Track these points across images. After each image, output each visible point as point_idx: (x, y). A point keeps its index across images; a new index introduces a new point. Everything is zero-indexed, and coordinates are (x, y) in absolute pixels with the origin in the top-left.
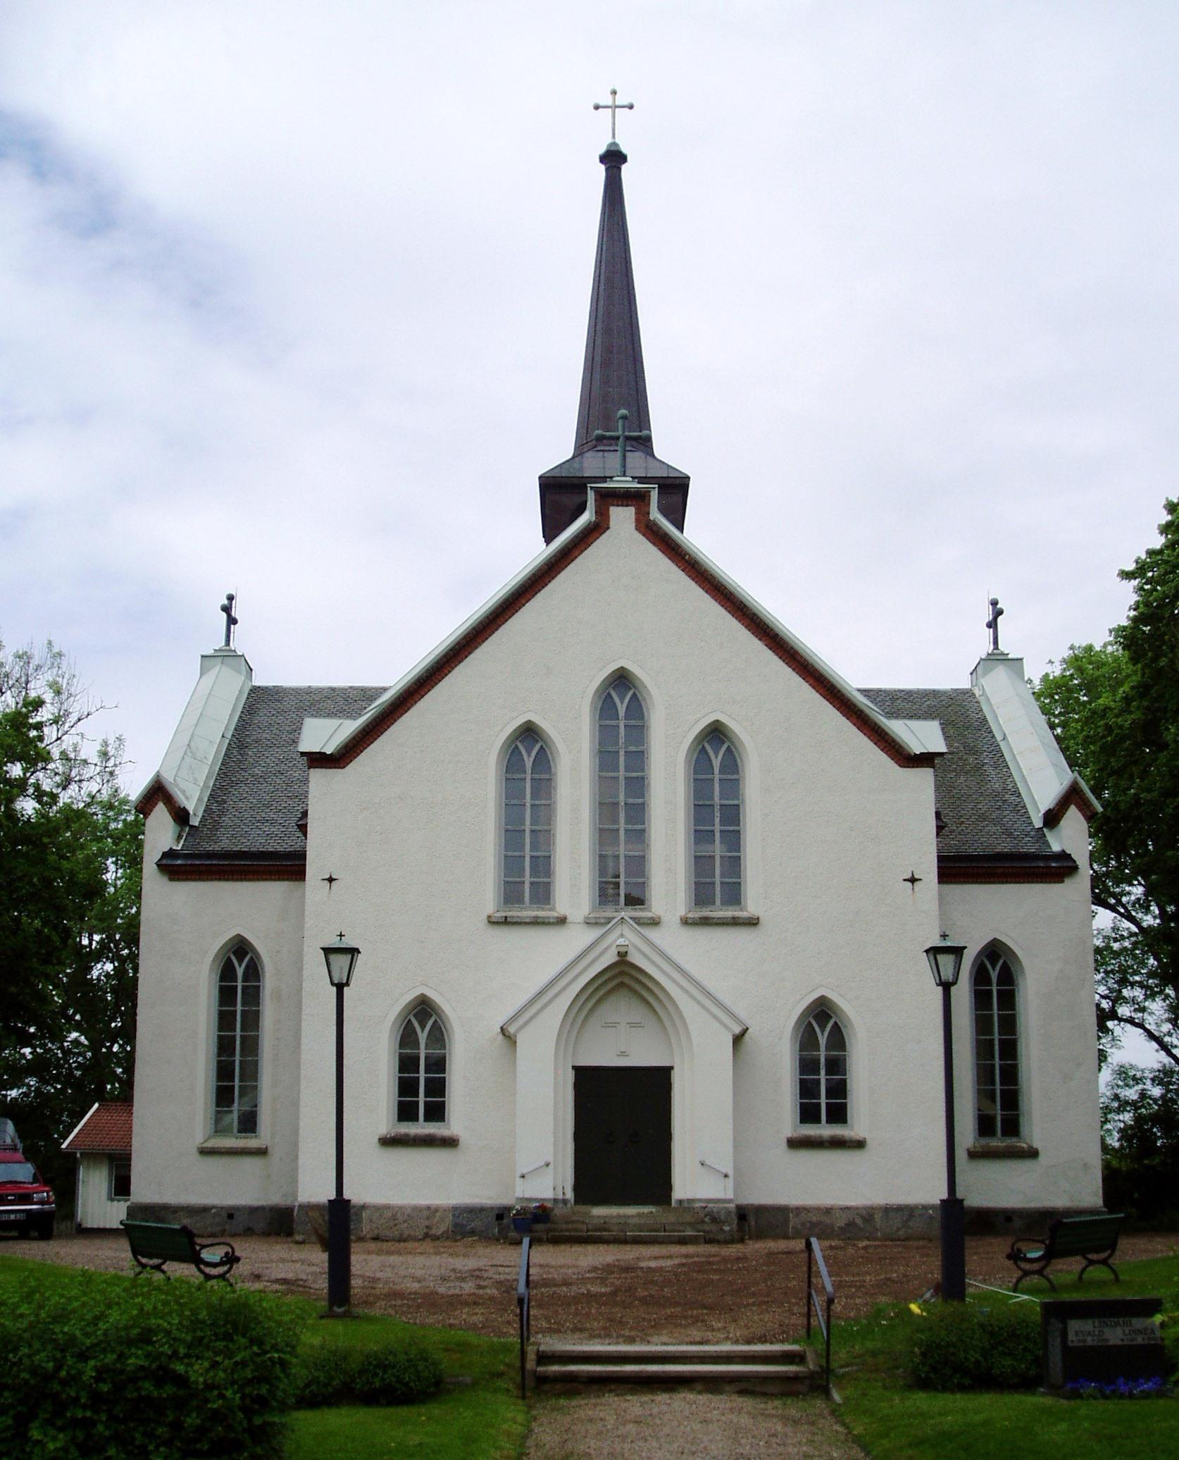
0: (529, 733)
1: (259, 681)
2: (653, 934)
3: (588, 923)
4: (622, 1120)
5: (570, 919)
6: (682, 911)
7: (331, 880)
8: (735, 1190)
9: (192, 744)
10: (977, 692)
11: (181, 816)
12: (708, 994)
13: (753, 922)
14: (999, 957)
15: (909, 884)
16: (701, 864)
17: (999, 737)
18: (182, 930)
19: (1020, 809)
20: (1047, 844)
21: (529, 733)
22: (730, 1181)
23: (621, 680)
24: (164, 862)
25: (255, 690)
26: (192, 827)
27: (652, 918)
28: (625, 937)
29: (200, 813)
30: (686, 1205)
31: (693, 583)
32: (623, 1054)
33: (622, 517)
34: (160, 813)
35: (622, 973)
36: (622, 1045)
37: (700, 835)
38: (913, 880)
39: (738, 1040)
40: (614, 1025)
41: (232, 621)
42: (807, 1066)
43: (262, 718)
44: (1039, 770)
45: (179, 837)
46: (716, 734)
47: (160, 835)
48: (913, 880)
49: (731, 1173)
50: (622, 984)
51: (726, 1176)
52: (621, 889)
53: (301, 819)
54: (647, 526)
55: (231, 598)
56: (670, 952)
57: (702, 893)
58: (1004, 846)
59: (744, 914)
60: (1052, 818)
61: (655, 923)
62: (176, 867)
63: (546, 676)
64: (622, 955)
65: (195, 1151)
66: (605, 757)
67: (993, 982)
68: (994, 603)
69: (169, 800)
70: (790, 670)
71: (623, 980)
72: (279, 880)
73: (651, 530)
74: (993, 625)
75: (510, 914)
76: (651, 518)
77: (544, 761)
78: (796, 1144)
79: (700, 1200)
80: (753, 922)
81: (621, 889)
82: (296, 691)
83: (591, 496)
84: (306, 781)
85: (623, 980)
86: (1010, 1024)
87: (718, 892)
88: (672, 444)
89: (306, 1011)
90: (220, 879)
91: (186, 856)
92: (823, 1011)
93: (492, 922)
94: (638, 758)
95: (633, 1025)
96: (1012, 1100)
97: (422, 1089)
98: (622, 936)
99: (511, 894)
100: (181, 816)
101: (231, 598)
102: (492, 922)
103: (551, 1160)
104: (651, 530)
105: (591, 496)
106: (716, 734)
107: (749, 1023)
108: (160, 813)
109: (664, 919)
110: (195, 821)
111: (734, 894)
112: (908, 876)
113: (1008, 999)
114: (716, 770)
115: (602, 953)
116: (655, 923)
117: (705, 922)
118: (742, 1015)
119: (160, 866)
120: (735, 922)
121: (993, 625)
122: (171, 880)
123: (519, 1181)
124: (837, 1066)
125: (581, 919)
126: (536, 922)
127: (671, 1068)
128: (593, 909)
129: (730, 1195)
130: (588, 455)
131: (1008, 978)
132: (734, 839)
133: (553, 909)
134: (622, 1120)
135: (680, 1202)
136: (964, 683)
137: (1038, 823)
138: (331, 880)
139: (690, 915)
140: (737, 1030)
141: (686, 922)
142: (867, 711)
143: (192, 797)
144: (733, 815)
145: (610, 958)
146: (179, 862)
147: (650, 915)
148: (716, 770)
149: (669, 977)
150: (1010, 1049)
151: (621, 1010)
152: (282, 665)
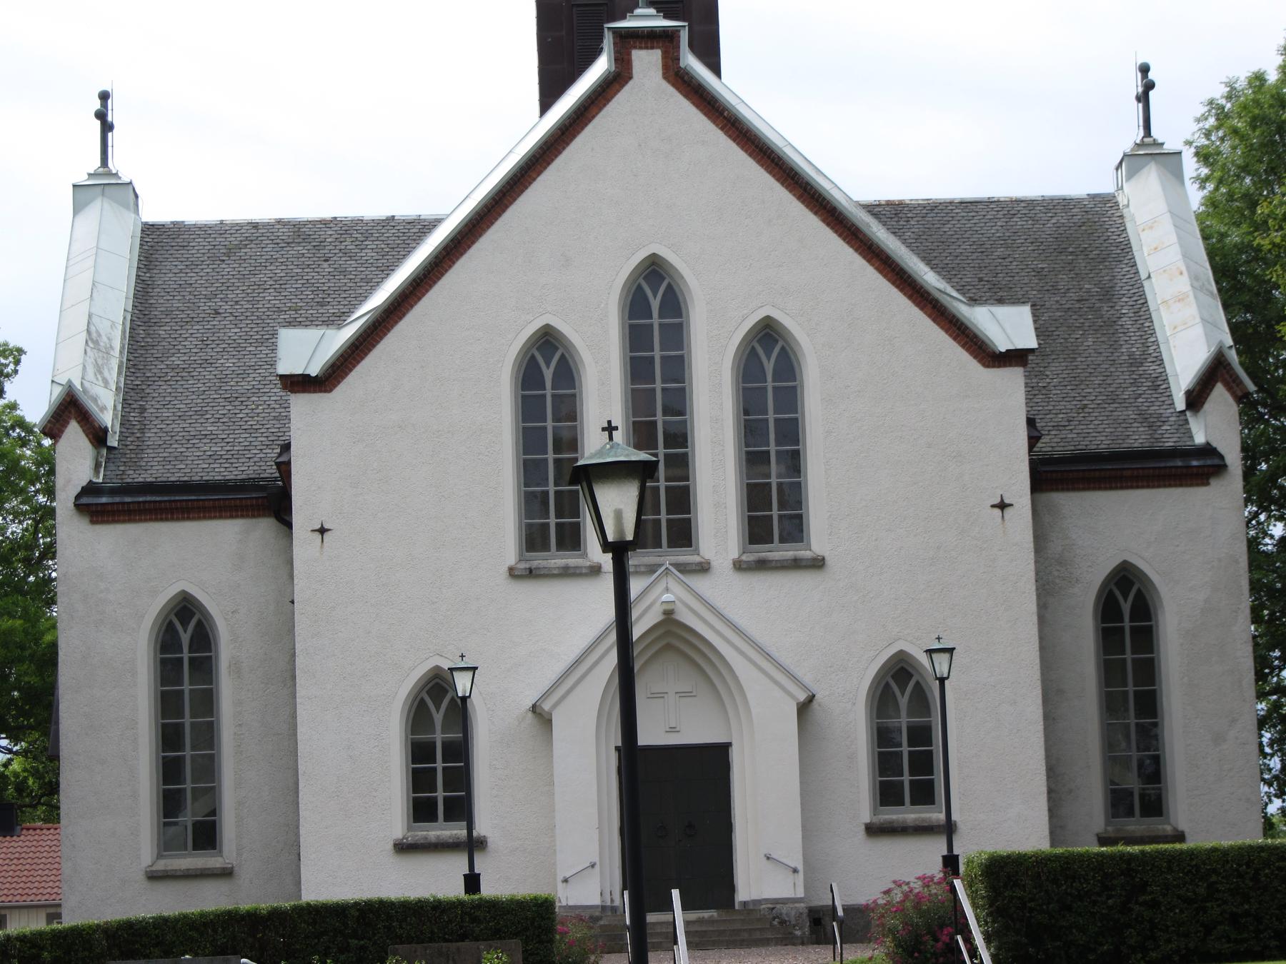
0: (547, 343)
1: (156, 211)
2: (700, 584)
4: (674, 810)
6: (734, 554)
7: (322, 531)
8: (806, 888)
9: (93, 329)
10: (1122, 200)
11: (98, 436)
12: (768, 656)
13: (818, 564)
14: (1132, 584)
15: (997, 512)
16: (755, 497)
17: (1143, 275)
19: (1160, 383)
20: (1191, 437)
22: (801, 875)
24: (84, 500)
25: (150, 230)
26: (111, 449)
27: (700, 563)
29: (117, 429)
32: (673, 730)
33: (647, 62)
35: (668, 633)
37: (753, 460)
38: (1002, 506)
39: (804, 708)
41: (107, 127)
42: (883, 736)
44: (1188, 330)
45: (97, 466)
47: (76, 463)
48: (1002, 506)
49: (800, 868)
50: (669, 647)
51: (795, 871)
53: (280, 455)
55: (104, 97)
56: (719, 603)
57: (757, 531)
58: (1138, 439)
59: (806, 554)
61: (703, 568)
62: (100, 505)
64: (668, 613)
65: (141, 876)
66: (638, 369)
67: (1127, 610)
68: (1144, 69)
70: (851, 250)
73: (682, 78)
74: (1144, 98)
75: (535, 564)
76: (682, 65)
77: (568, 373)
78: (873, 830)
79: (767, 900)
80: (818, 564)
83: (608, 42)
84: (284, 419)
86: (1148, 671)
87: (774, 515)
89: (301, 692)
90: (156, 520)
91: (113, 491)
92: (902, 669)
94: (678, 368)
96: (1154, 771)
97: (440, 771)
98: (667, 590)
100: (98, 436)
101: (104, 97)
102: (513, 573)
103: (597, 860)
105: (608, 42)
107: (815, 688)
109: (714, 564)
110: (113, 441)
111: (795, 529)
112: (997, 501)
113: (1146, 637)
114: (769, 378)
116: (703, 568)
117: (762, 565)
118: (807, 679)
120: (797, 565)
121: (1144, 98)
122: (93, 522)
123: (560, 886)
126: (567, 573)
127: (728, 745)
129: (800, 893)
131: (1144, 609)
132: (794, 462)
133: (585, 555)
134: (674, 810)
135: (745, 903)
136: (1105, 185)
137: (1180, 404)
139: (744, 558)
140: (802, 697)
141: (739, 566)
142: (944, 300)
143: (106, 404)
144: (791, 432)
146: (104, 500)
147: (696, 559)
148: (769, 378)
150: (1149, 704)
152: (186, 192)
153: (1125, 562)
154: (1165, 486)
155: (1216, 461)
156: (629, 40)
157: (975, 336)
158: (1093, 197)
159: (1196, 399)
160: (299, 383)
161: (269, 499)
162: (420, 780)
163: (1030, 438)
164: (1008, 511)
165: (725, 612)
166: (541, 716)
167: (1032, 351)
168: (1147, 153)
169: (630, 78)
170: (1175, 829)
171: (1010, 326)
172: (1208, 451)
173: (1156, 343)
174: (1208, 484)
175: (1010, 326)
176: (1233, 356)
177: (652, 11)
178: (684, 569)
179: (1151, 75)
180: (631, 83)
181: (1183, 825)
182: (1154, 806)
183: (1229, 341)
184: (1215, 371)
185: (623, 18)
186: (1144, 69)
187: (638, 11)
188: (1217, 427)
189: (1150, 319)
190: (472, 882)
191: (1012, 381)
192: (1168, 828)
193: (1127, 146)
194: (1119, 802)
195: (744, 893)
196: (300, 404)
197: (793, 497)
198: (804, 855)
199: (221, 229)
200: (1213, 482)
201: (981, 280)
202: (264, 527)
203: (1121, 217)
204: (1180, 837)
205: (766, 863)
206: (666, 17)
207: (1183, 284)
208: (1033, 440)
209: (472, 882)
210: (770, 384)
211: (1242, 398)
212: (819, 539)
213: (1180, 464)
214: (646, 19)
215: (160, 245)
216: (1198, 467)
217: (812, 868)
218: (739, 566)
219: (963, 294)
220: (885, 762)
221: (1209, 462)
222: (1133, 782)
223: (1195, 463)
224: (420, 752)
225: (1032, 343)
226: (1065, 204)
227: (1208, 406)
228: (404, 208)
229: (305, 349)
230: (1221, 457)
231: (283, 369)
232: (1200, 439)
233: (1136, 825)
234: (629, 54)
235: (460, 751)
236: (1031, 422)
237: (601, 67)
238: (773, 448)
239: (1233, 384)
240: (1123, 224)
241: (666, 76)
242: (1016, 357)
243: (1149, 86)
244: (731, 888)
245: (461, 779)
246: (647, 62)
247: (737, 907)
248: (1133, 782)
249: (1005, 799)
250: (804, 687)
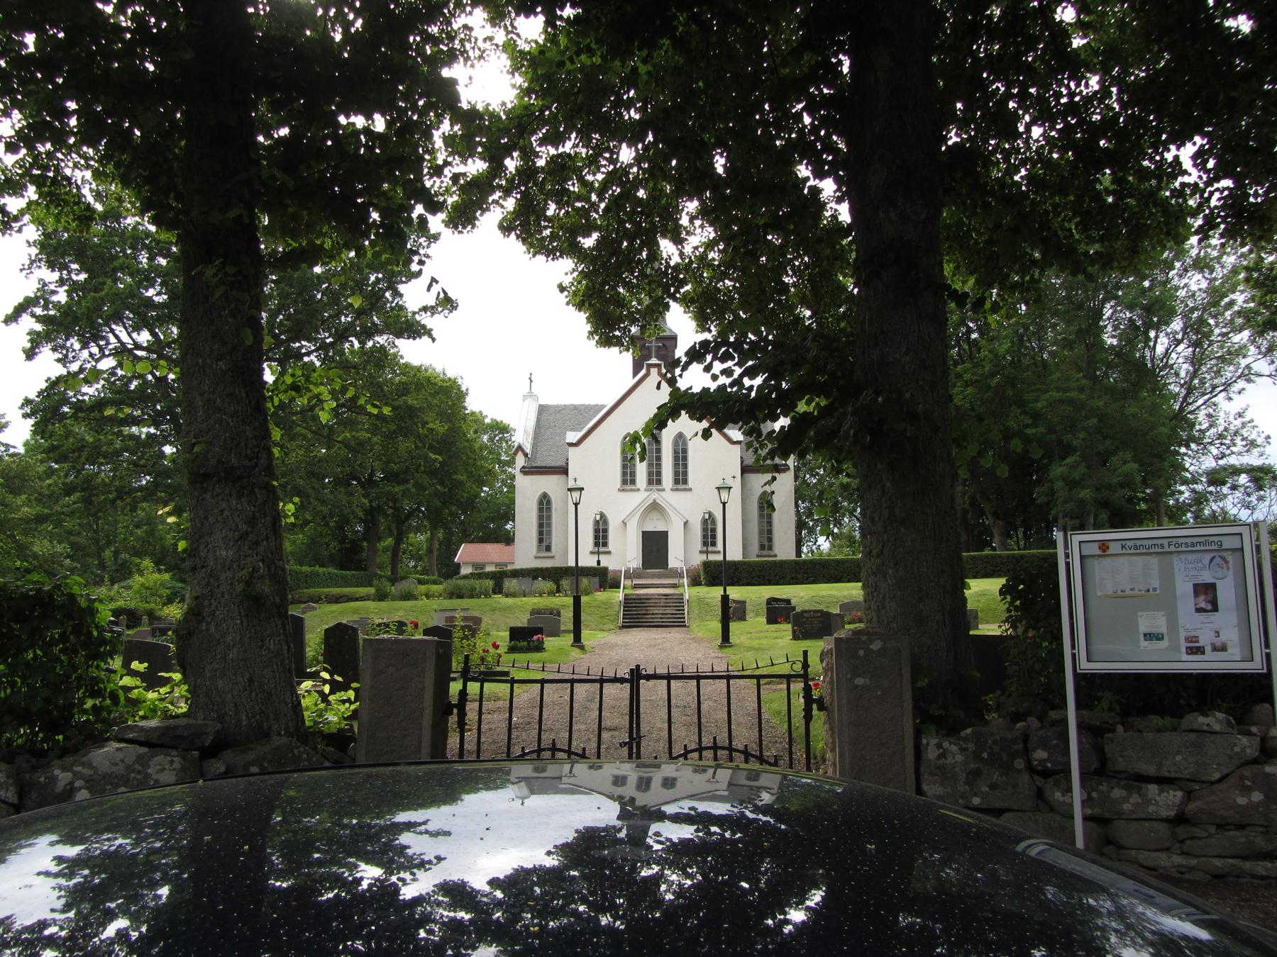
1: (542, 402)
4: (654, 546)
11: (526, 455)
16: (676, 473)
18: (528, 490)
25: (540, 406)
28: (655, 496)
33: (654, 371)
34: (520, 453)
36: (655, 525)
37: (676, 465)
39: (686, 523)
42: (705, 530)
43: (544, 417)
47: (520, 461)
52: (655, 478)
57: (676, 482)
62: (526, 471)
67: (766, 504)
69: (523, 451)
71: (655, 507)
81: (655, 478)
82: (554, 406)
85: (655, 507)
87: (681, 478)
96: (770, 540)
97: (601, 536)
99: (624, 482)
100: (526, 455)
108: (520, 453)
111: (685, 482)
126: (632, 490)
132: (685, 466)
134: (654, 546)
143: (528, 449)
151: (655, 515)
156: (650, 366)
160: (571, 445)
161: (563, 471)
162: (596, 537)
166: (625, 524)
182: (770, 548)
190: (599, 562)
191: (737, 448)
194: (762, 547)
196: (571, 449)
197: (685, 474)
199: (557, 406)
202: (564, 477)
205: (676, 558)
209: (599, 562)
212: (691, 484)
214: (654, 361)
215: (542, 409)
220: (705, 537)
222: (766, 543)
224: (596, 531)
228: (600, 403)
229: (572, 437)
231: (568, 440)
233: (765, 552)
235: (605, 531)
237: (643, 372)
242: (739, 442)
245: (605, 537)
246: (654, 371)
248: (766, 543)
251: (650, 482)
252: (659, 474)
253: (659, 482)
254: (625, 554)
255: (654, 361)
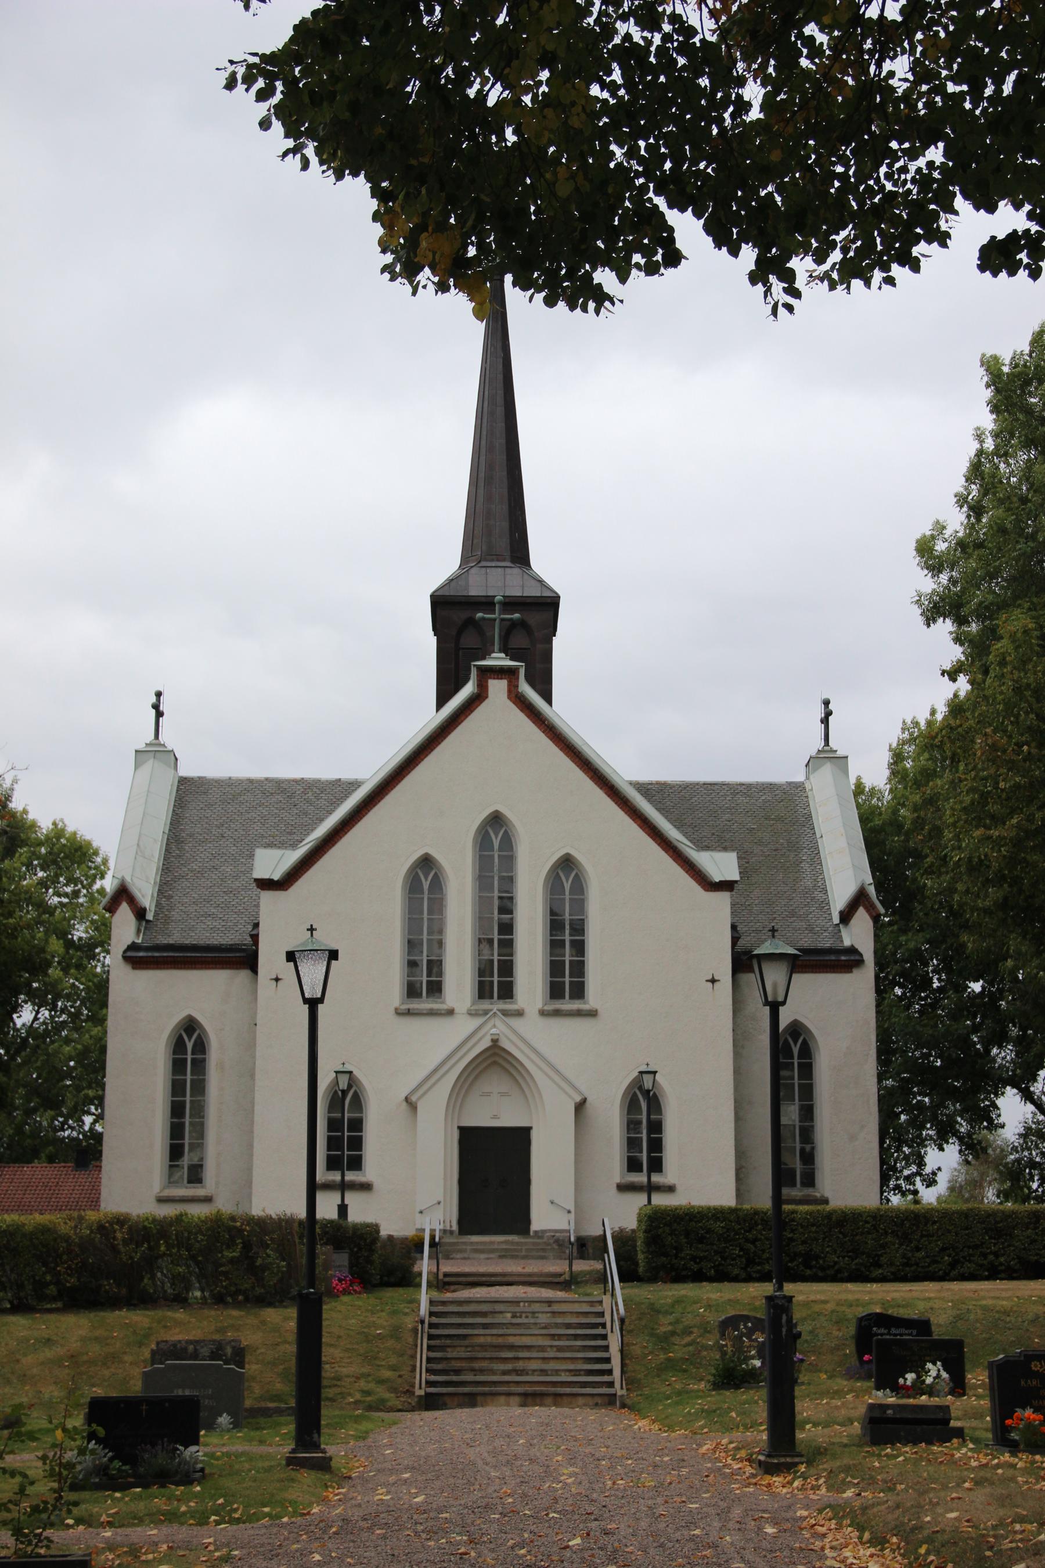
0: (426, 862)
1: (187, 769)
3: (472, 1014)
4: (493, 1169)
5: (456, 1011)
6: (539, 1005)
7: (277, 980)
10: (808, 786)
11: (140, 913)
12: (557, 1071)
13: (593, 1014)
14: (800, 1035)
15: (710, 984)
16: (555, 968)
17: (818, 836)
18: (144, 1011)
19: (824, 905)
21: (426, 862)
22: (572, 1216)
23: (496, 820)
24: (129, 954)
25: (183, 781)
26: (148, 921)
28: (498, 1027)
29: (153, 909)
30: (538, 1234)
31: (551, 743)
32: (495, 1117)
33: (498, 688)
34: (124, 909)
35: (495, 1054)
37: (555, 945)
39: (580, 1107)
40: (488, 1094)
41: (159, 714)
45: (138, 931)
46: (567, 863)
47: (124, 929)
48: (713, 981)
49: (573, 1210)
50: (495, 1063)
51: (569, 1212)
52: (496, 982)
54: (516, 696)
55: (159, 694)
57: (555, 991)
59: (585, 1007)
60: (846, 917)
61: (520, 1014)
62: (139, 958)
63: (437, 821)
64: (495, 1041)
65: (153, 1200)
68: (827, 703)
69: (132, 900)
71: (495, 1060)
72: (223, 968)
73: (519, 699)
74: (825, 721)
75: (411, 1006)
76: (520, 690)
77: (438, 884)
79: (550, 1231)
80: (593, 1014)
81: (496, 982)
83: (474, 673)
85: (495, 1060)
87: (567, 981)
88: (550, 559)
93: (399, 1013)
95: (503, 1094)
98: (494, 1026)
99: (412, 991)
100: (140, 913)
101: (159, 694)
102: (399, 1013)
103: (441, 1199)
104: (519, 699)
105: (474, 673)
106: (567, 863)
107: (587, 1095)
108: (124, 910)
109: (527, 1011)
110: (150, 916)
111: (579, 991)
114: (567, 893)
115: (481, 1039)
117: (557, 1013)
118: (583, 1089)
119: (126, 958)
120: (579, 1013)
121: (825, 721)
122: (134, 968)
123: (418, 1215)
124: (656, 1127)
125: (464, 1010)
126: (432, 1013)
128: (473, 1004)
130: (473, 571)
132: (579, 947)
133: (443, 1002)
134: (493, 1169)
135: (536, 1232)
137: (836, 920)
138: (277, 980)
139: (546, 1008)
140: (578, 1099)
141: (543, 1013)
142: (681, 847)
143: (146, 895)
144: (579, 928)
145: (486, 1043)
146: (141, 954)
148: (567, 893)
149: (528, 1057)
151: (494, 1083)
153: (796, 1020)
154: (823, 972)
155: (857, 958)
157: (700, 871)
158: (789, 784)
159: (846, 917)
160: (266, 884)
161: (244, 958)
163: (733, 938)
164: (716, 984)
165: (532, 1043)
166: (411, 1104)
167: (736, 882)
168: (827, 756)
169: (487, 697)
170: (823, 1196)
171: (723, 865)
172: (853, 950)
173: (823, 879)
174: (851, 972)
175: (723, 865)
176: (872, 890)
177: (503, 655)
178: (506, 1013)
179: (831, 707)
180: (486, 701)
181: (828, 1193)
183: (870, 879)
184: (859, 899)
185: (484, 658)
186: (827, 703)
187: (494, 655)
188: (860, 935)
189: (821, 864)
191: (723, 900)
192: (818, 1195)
193: (814, 753)
194: (781, 1177)
195: (536, 1225)
196: (267, 898)
197: (579, 968)
198: (576, 1202)
200: (855, 971)
201: (713, 834)
202: (244, 975)
203: (807, 797)
204: (826, 1201)
205: (550, 1206)
206: (511, 659)
207: (843, 843)
208: (735, 940)
210: (567, 896)
211: (876, 919)
212: (593, 998)
213: (833, 958)
214: (498, 659)
215: (188, 790)
216: (844, 961)
217: (579, 1211)
218: (543, 1013)
219: (694, 844)
221: (852, 958)
223: (843, 958)
225: (736, 877)
226: (771, 787)
227: (853, 921)
228: (346, 774)
229: (272, 863)
230: (861, 955)
232: (847, 943)
234: (487, 682)
235: (357, 1125)
236: (734, 927)
237: (468, 690)
238: (567, 938)
239: (870, 908)
240: (807, 801)
241: (509, 698)
242: (726, 886)
243: (828, 714)
244: (528, 1222)
246: (498, 688)
247: (531, 1233)
249: (704, 1174)
250: (580, 1093)
251: (483, 991)
252: (507, 968)
253: (507, 992)
254: (409, 1189)
255: (498, 659)
